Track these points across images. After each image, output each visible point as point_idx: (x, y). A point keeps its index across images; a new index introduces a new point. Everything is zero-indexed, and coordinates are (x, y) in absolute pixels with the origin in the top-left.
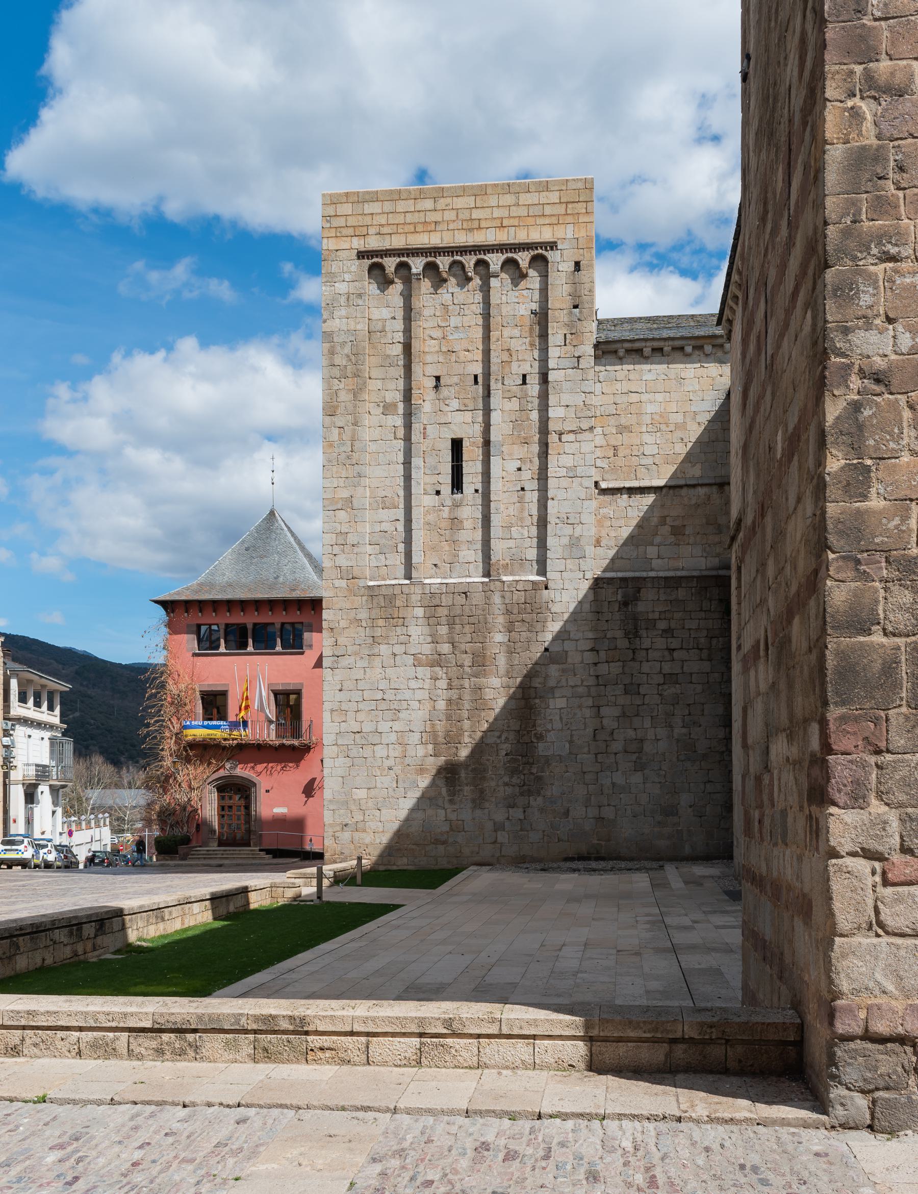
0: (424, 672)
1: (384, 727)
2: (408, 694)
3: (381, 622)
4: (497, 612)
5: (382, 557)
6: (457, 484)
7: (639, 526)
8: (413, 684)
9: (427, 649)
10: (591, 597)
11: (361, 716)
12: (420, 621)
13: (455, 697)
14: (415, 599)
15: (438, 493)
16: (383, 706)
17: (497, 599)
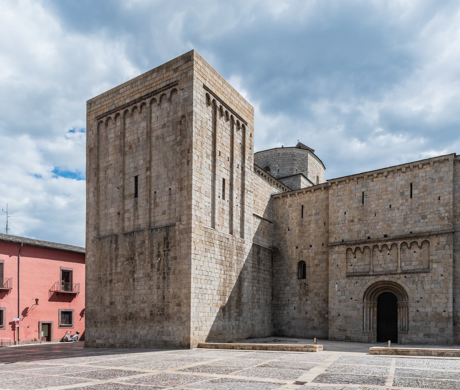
0: (218, 266)
1: (208, 287)
2: (214, 275)
3: (208, 243)
4: (235, 248)
5: (205, 216)
6: (224, 198)
7: (258, 229)
8: (216, 271)
9: (219, 257)
10: (252, 250)
11: (202, 281)
12: (218, 246)
13: (225, 278)
14: (217, 236)
15: (219, 197)
16: (208, 278)
17: (235, 244)
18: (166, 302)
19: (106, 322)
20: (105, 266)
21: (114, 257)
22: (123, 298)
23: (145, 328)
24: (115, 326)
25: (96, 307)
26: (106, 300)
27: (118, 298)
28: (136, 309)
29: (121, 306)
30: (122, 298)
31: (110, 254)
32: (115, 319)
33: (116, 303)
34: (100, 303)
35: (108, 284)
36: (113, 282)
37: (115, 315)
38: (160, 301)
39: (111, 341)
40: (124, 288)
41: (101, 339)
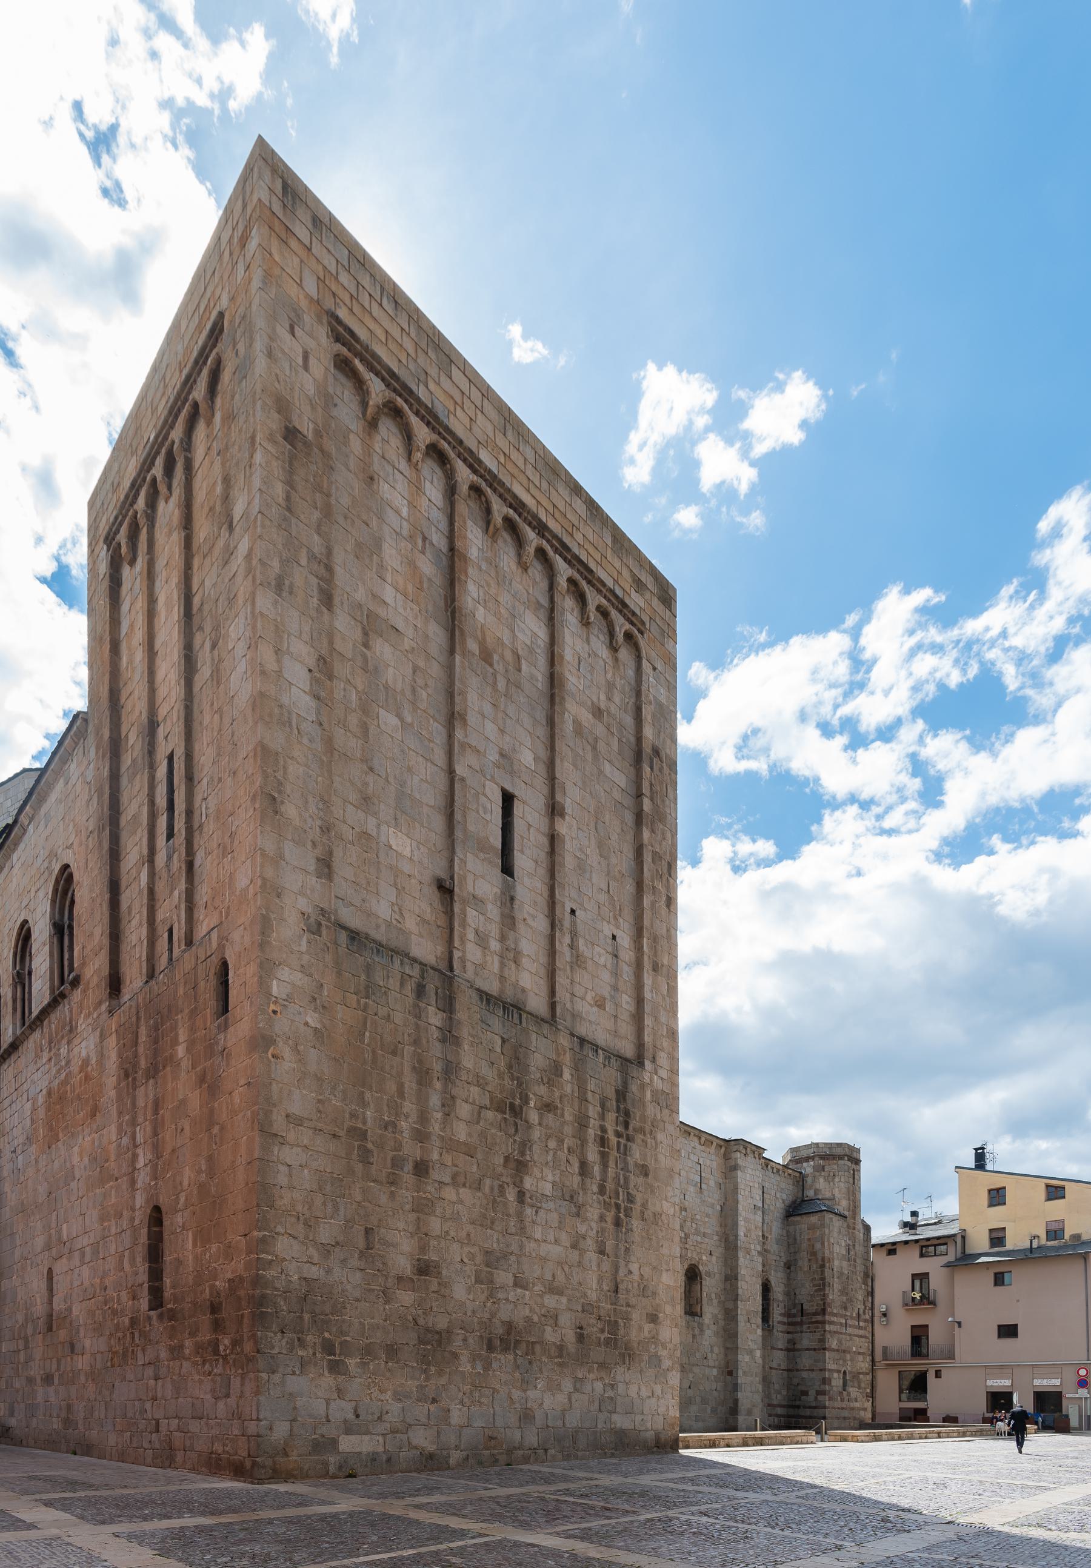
18: (621, 1302)
19: (392, 1352)
20: (391, 1086)
21: (437, 1067)
22: (479, 1259)
23: (559, 1385)
24: (440, 1373)
25: (337, 1270)
26: (395, 1245)
27: (456, 1252)
28: (527, 1312)
29: (469, 1290)
30: (472, 1257)
31: (416, 1042)
32: (439, 1343)
33: (444, 1272)
34: (362, 1254)
35: (407, 1177)
36: (435, 1175)
37: (442, 1323)
38: (606, 1296)
39: (422, 1439)
40: (484, 1216)
41: (367, 1432)
